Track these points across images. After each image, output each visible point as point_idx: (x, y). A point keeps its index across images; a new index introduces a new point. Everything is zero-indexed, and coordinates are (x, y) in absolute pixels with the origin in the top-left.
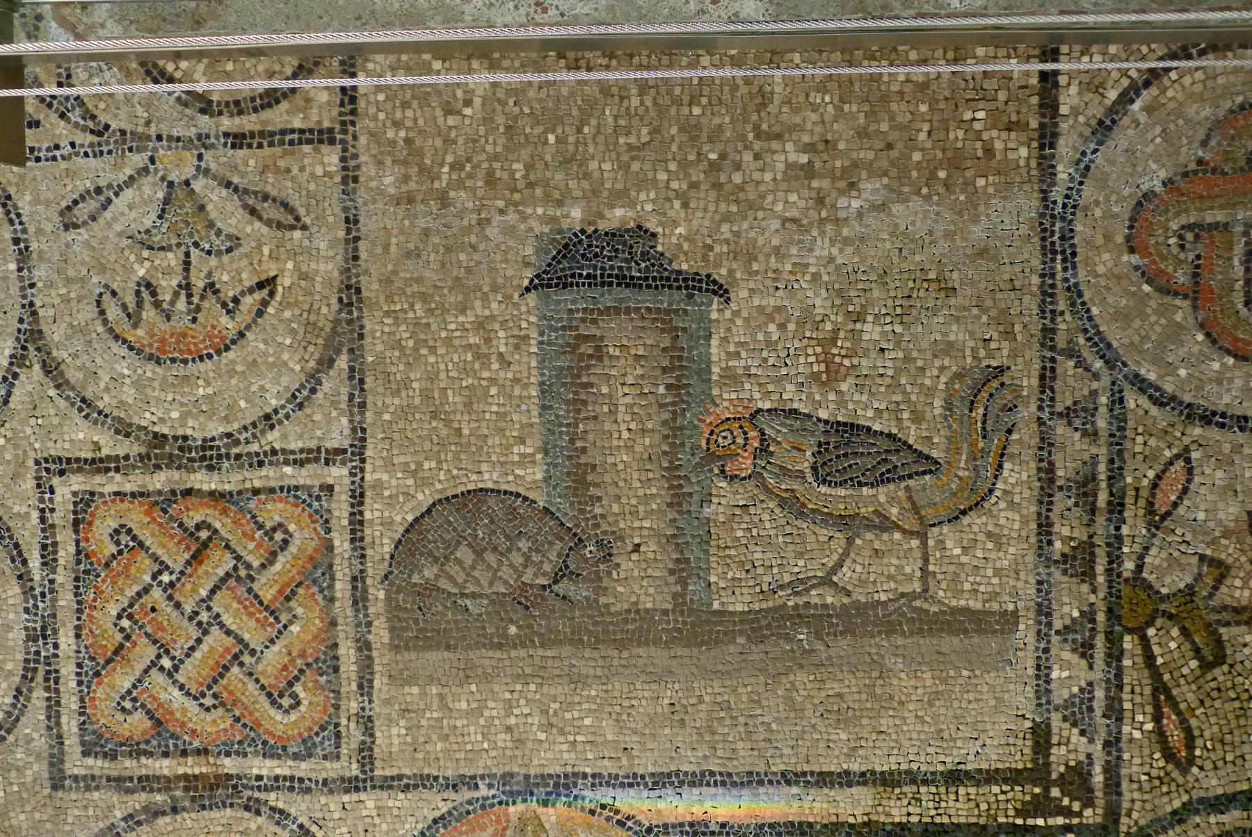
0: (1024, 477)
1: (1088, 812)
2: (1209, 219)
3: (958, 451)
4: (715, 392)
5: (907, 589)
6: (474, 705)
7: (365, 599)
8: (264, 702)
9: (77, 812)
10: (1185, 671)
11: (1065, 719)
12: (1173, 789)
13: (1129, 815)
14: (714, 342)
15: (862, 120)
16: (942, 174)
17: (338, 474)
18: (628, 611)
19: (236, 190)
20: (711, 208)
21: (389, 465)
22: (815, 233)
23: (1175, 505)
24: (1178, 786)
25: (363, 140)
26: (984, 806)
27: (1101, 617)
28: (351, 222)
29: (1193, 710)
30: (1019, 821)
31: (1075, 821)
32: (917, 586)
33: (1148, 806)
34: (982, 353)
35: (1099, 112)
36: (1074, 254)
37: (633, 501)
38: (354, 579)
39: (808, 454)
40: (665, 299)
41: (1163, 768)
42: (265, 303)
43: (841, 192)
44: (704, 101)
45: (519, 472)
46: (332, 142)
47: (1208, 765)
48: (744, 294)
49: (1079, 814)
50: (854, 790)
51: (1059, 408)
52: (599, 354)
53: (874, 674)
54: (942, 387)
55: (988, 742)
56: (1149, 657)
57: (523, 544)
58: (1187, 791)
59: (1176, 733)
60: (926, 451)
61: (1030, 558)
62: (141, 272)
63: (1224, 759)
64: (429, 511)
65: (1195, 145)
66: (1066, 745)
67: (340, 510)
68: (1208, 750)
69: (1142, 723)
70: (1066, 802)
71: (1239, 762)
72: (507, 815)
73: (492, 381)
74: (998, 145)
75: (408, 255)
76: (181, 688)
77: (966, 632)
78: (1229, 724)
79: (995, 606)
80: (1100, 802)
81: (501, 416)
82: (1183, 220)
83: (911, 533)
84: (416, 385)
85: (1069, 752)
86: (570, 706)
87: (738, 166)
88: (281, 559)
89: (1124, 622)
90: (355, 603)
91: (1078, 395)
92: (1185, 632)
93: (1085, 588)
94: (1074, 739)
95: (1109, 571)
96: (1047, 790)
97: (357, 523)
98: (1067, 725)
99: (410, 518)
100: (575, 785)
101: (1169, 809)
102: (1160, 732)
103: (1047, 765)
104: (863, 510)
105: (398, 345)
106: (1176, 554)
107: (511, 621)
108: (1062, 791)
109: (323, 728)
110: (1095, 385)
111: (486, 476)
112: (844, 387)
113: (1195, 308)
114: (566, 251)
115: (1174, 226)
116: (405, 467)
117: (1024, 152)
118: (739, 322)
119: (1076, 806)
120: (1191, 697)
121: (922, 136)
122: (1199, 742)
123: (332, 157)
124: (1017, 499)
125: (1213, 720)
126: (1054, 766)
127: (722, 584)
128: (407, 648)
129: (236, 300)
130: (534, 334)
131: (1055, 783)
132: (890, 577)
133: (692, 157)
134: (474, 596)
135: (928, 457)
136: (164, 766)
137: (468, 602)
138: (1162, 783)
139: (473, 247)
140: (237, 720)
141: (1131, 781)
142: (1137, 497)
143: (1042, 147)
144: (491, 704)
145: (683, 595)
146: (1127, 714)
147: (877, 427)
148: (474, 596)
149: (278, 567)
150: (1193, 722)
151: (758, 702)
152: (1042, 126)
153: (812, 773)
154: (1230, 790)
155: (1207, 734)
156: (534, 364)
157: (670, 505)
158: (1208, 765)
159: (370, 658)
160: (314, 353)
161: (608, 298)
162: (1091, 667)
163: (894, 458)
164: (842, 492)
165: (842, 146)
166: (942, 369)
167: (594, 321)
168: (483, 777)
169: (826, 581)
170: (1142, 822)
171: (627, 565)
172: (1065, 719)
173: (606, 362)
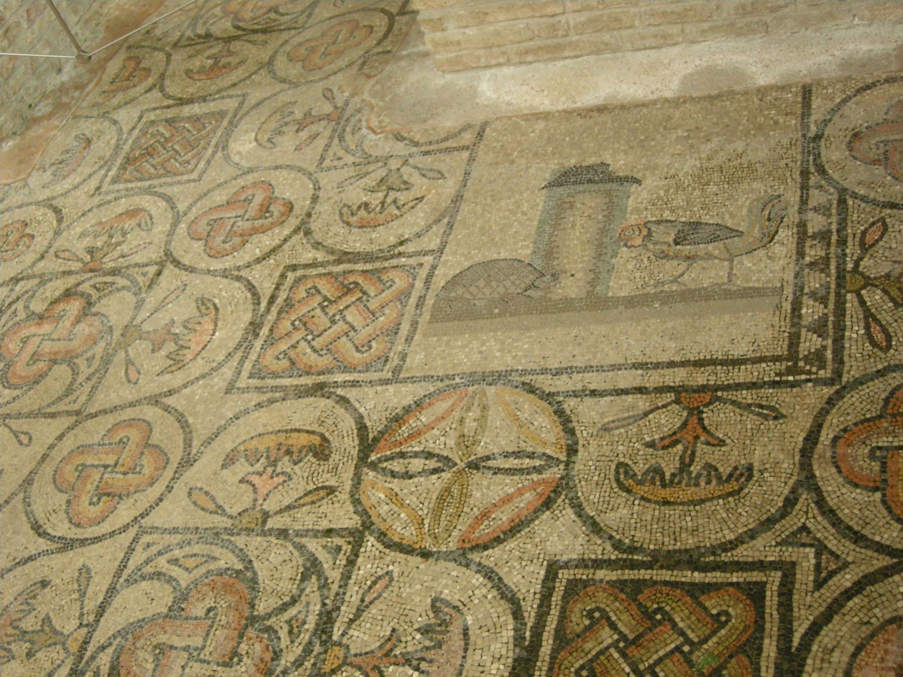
0: (790, 234)
1: (822, 372)
2: (892, 138)
3: (754, 227)
4: (628, 216)
5: (720, 281)
6: (465, 343)
7: (422, 304)
8: (353, 350)
9: (232, 404)
10: (885, 307)
11: (808, 331)
13: (849, 372)
14: (631, 199)
15: (715, 120)
16: (753, 132)
17: (429, 259)
18: (561, 299)
19: (419, 169)
20: (638, 153)
21: (455, 253)
22: (688, 157)
23: (877, 241)
25: (482, 147)
26: (756, 374)
27: (833, 286)
28: (467, 174)
30: (778, 379)
31: (813, 377)
32: (726, 280)
34: (769, 190)
35: (831, 106)
36: (819, 154)
37: (576, 258)
38: (420, 297)
39: (673, 235)
40: (608, 186)
42: (417, 204)
43: (702, 143)
44: (642, 122)
45: (519, 251)
46: (468, 149)
48: (649, 181)
49: (816, 373)
50: (676, 369)
51: (810, 206)
52: (572, 207)
53: (696, 318)
54: (747, 204)
55: (761, 344)
56: (862, 303)
57: (512, 278)
60: (736, 228)
61: (792, 266)
62: (365, 199)
64: (468, 268)
65: (882, 114)
67: (423, 273)
70: (808, 367)
72: (467, 391)
73: (516, 221)
74: (781, 121)
75: (490, 182)
76: (312, 347)
77: (752, 297)
79: (770, 285)
81: (516, 232)
82: (878, 139)
83: (724, 260)
84: (478, 225)
86: (518, 340)
87: (653, 140)
88: (387, 292)
89: (847, 288)
90: (417, 306)
91: (820, 201)
92: (885, 291)
93: (823, 275)
95: (838, 268)
96: (796, 364)
97: (430, 275)
98: (810, 333)
99: (458, 272)
100: (510, 375)
101: (875, 369)
103: (797, 352)
104: (699, 253)
105: (475, 213)
106: (879, 261)
107: (496, 308)
109: (379, 359)
110: (830, 197)
111: (502, 254)
112: (695, 209)
113: (886, 169)
114: (565, 174)
115: (873, 142)
116: (462, 255)
117: (794, 122)
118: (645, 191)
119: (814, 369)
120: (889, 319)
121: (744, 121)
123: (465, 155)
124: (785, 242)
127: (616, 286)
128: (437, 322)
129: (404, 205)
130: (541, 204)
131: (801, 360)
132: (710, 278)
133: (632, 139)
134: (480, 299)
135: (737, 231)
136: (286, 382)
137: (476, 302)
139: (521, 176)
140: (335, 359)
142: (854, 237)
143: (803, 119)
144: (475, 342)
145: (592, 291)
147: (711, 222)
148: (480, 299)
149: (384, 295)
151: (626, 333)
152: (803, 113)
153: (651, 363)
156: (539, 213)
157: (594, 258)
159: (416, 328)
160: (433, 218)
161: (581, 188)
162: (826, 307)
163: (718, 233)
164: (688, 247)
165: (705, 128)
166: (747, 198)
167: (573, 196)
168: (458, 375)
169: (675, 281)
170: (857, 376)
171: (566, 281)
172: (808, 331)
173: (575, 210)
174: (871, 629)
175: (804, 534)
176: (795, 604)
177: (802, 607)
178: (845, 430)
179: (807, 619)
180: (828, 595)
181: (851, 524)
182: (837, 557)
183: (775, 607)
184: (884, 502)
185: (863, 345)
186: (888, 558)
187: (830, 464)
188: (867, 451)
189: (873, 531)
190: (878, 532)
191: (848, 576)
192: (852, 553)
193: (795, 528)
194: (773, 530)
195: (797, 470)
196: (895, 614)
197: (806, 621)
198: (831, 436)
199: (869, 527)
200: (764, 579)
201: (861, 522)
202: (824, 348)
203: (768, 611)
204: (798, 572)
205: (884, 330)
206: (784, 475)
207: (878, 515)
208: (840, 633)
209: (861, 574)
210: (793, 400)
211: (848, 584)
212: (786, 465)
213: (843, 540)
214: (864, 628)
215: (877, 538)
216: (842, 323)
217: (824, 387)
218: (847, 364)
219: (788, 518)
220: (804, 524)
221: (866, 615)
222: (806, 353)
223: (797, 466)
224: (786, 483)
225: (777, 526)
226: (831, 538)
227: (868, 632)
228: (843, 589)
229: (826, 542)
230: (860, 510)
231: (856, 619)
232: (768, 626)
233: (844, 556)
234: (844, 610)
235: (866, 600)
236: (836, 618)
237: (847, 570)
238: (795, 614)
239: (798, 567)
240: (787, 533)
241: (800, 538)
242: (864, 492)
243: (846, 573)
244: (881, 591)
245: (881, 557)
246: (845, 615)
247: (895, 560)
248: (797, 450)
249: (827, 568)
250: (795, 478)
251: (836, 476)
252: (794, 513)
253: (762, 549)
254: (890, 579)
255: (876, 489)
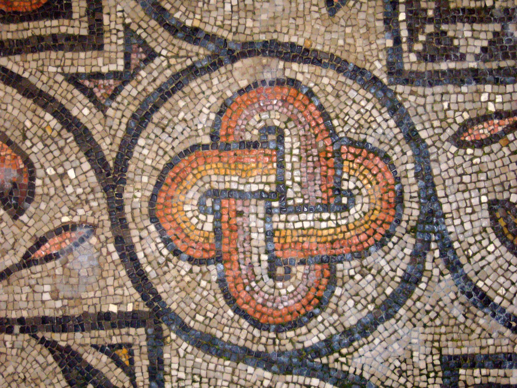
1: (413, 57)
11: (496, 34)
12: (436, 131)
13: (412, 93)
24: (439, 135)
29: (507, 146)
31: (405, 47)
33: (420, 110)
41: (455, 122)
47: (458, 160)
49: (410, 51)
58: (434, 142)
59: (486, 131)
63: (465, 174)
66: (472, 37)
68: (471, 160)
69: (494, 101)
70: (422, 38)
71: (462, 187)
78: (496, 177)
80: (422, 67)
85: (466, 39)
94: (478, 43)
96: (430, 21)
98: (490, 36)
102: (486, 118)
108: (430, 34)
119: (418, 47)
122: (478, 152)
125: (499, 163)
126: (453, 26)
131: (437, 28)
138: (441, 121)
141: (442, 94)
146: (502, 88)
150: (495, 147)
154: (437, 181)
155: (485, 159)
158: (458, 160)
170: (406, 105)
172: (496, 34)
174: (17, 141)
175: (144, 56)
176: (43, 55)
177: (40, 63)
178: (310, 94)
179: (25, 70)
180: (59, 92)
181: (162, 110)
182: (112, 97)
183: (37, 32)
184: (194, 148)
185: (465, 110)
186: (114, 155)
187: (252, 80)
188: (277, 123)
189: (152, 136)
190: (150, 142)
191: (86, 111)
192: (119, 114)
193: (153, 45)
194: (147, 18)
195: (242, 38)
196: (37, 166)
197: (22, 69)
198: (300, 77)
199: (158, 131)
200: (75, 16)
201: (165, 122)
202: (463, 57)
203: (31, 24)
204: (89, 53)
205: (493, 139)
206: (235, 24)
207: (177, 142)
208: (10, 108)
209: (89, 126)
210: (361, 23)
211: (75, 112)
212: (250, 23)
213: (137, 102)
214: (17, 133)
215: (141, 142)
216: (508, 80)
217: (384, 63)
218: (429, 91)
219: (166, 34)
220: (160, 55)
221: (35, 134)
222: (451, 34)
223: (250, 39)
224: (221, 27)
225: (153, 23)
226: (140, 88)
227: (13, 139)
228: (68, 106)
229: (134, 83)
230: (184, 120)
231: (28, 124)
232: (13, 27)
233: (114, 105)
234: (40, 112)
235: (55, 134)
236: (29, 102)
237: (94, 110)
238: (30, 57)
239: (95, 53)
240: (144, 35)
241: (137, 52)
242: (210, 124)
243: (90, 109)
244: (67, 150)
245: (115, 147)
246: (34, 111)
247: (111, 164)
248: (275, 36)
249: (95, 86)
250: (230, 37)
251: (235, 89)
252: (175, 41)
253: (119, 8)
254: (84, 159)
255: (214, 136)
